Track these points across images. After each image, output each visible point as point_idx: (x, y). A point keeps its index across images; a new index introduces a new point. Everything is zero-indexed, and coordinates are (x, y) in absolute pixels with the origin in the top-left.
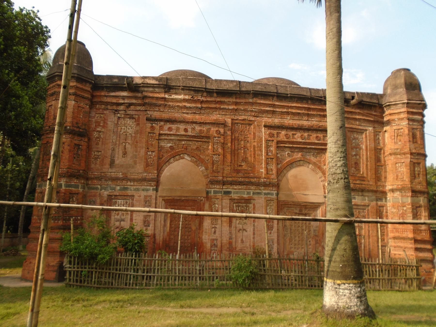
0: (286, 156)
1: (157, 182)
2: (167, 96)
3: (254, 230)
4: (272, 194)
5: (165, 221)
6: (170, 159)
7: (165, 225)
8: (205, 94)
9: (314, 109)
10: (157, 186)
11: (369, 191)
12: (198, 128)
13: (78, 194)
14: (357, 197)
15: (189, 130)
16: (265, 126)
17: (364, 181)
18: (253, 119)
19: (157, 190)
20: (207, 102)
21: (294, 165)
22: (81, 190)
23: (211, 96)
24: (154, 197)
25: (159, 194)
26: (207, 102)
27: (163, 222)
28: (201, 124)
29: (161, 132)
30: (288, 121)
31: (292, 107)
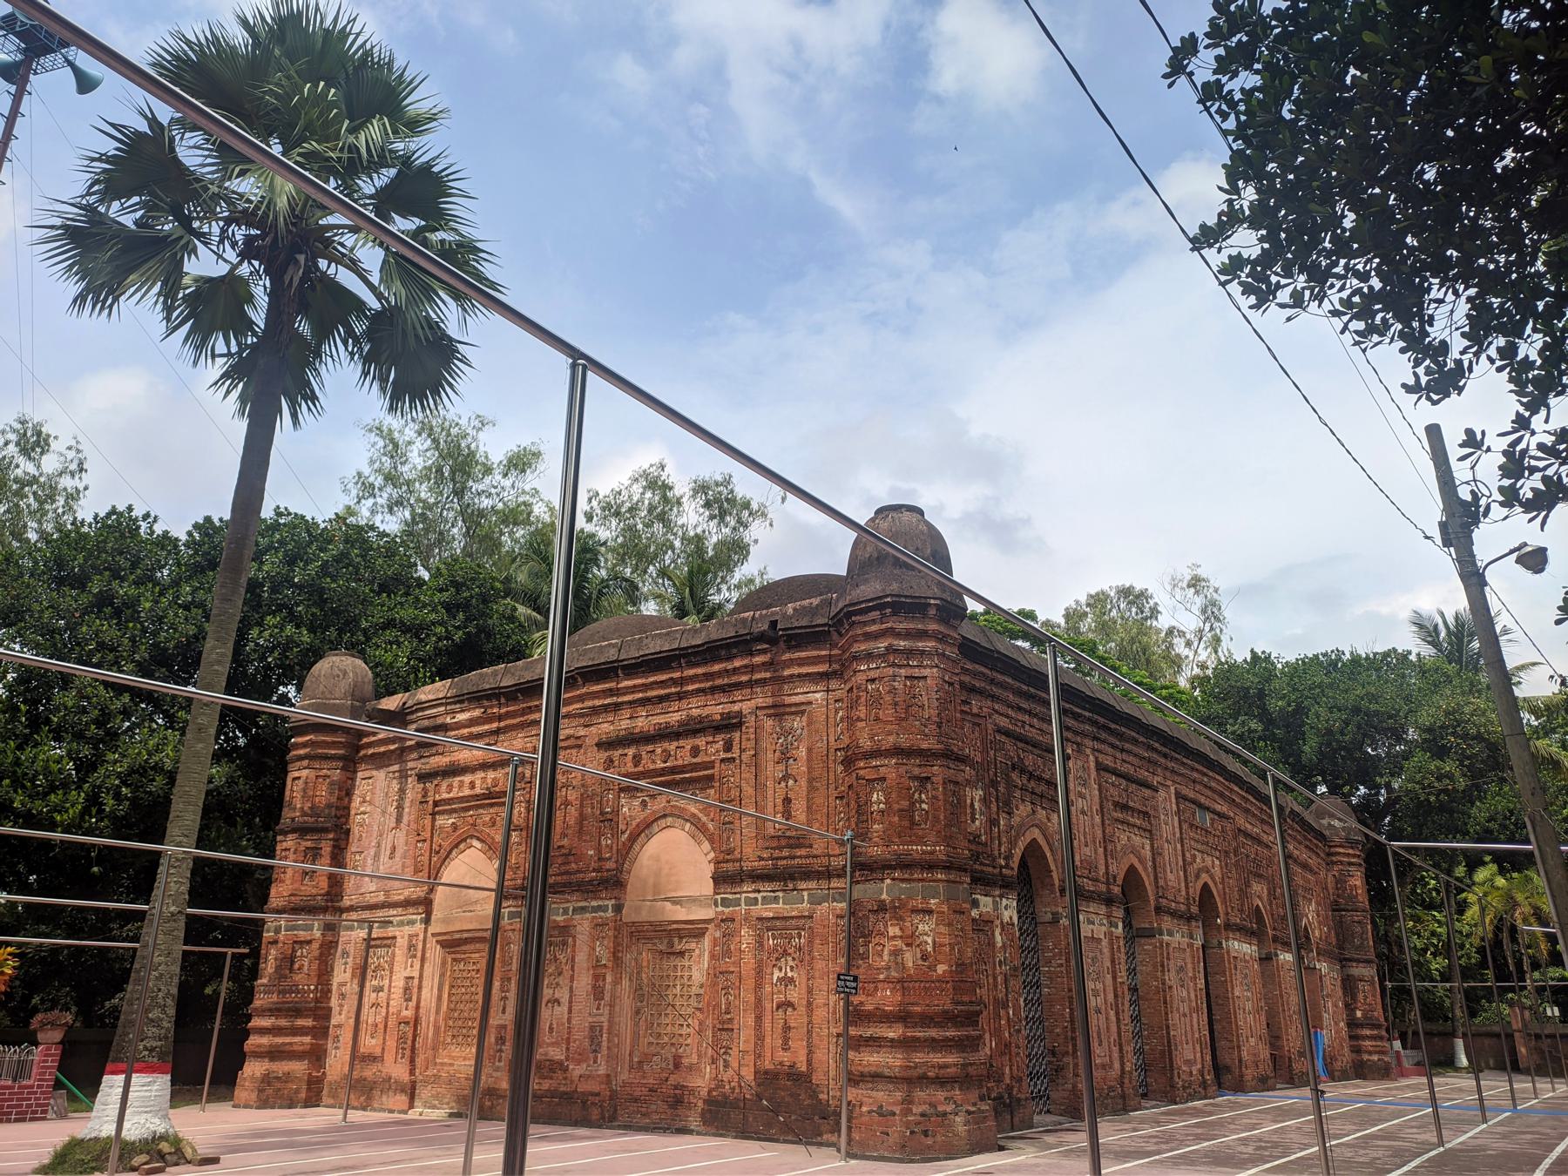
0: (630, 809)
1: (426, 904)
2: (448, 720)
3: (570, 1002)
4: (603, 909)
5: (440, 989)
6: (450, 852)
7: (440, 998)
8: (503, 700)
9: (693, 679)
10: (429, 913)
11: (807, 875)
12: (491, 775)
13: (309, 942)
14: (781, 894)
15: (478, 783)
16: (599, 745)
17: (800, 846)
18: (582, 733)
19: (427, 921)
20: (508, 715)
21: (655, 828)
22: (317, 934)
23: (515, 699)
24: (421, 937)
25: (431, 930)
26: (508, 715)
27: (435, 991)
28: (484, 766)
29: (437, 797)
30: (644, 721)
31: (646, 687)
